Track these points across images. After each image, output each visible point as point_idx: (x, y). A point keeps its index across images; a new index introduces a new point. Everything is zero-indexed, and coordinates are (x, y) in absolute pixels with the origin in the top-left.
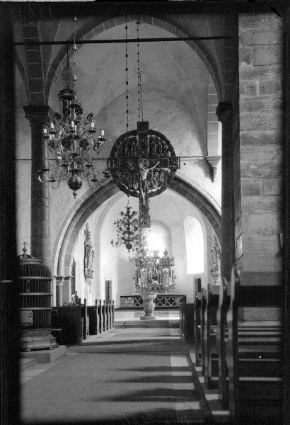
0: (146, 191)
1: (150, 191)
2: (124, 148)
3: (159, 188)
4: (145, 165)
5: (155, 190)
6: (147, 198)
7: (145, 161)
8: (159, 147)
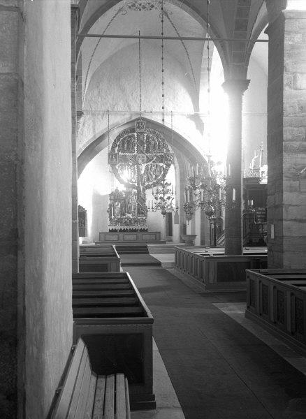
0: (143, 184)
1: (146, 184)
2: (123, 144)
3: (155, 181)
4: (143, 160)
5: (150, 183)
6: (144, 190)
7: (143, 157)
8: (155, 144)
